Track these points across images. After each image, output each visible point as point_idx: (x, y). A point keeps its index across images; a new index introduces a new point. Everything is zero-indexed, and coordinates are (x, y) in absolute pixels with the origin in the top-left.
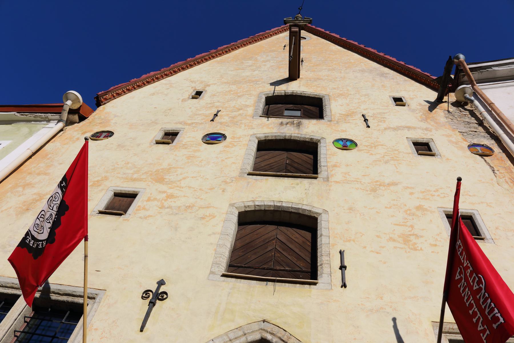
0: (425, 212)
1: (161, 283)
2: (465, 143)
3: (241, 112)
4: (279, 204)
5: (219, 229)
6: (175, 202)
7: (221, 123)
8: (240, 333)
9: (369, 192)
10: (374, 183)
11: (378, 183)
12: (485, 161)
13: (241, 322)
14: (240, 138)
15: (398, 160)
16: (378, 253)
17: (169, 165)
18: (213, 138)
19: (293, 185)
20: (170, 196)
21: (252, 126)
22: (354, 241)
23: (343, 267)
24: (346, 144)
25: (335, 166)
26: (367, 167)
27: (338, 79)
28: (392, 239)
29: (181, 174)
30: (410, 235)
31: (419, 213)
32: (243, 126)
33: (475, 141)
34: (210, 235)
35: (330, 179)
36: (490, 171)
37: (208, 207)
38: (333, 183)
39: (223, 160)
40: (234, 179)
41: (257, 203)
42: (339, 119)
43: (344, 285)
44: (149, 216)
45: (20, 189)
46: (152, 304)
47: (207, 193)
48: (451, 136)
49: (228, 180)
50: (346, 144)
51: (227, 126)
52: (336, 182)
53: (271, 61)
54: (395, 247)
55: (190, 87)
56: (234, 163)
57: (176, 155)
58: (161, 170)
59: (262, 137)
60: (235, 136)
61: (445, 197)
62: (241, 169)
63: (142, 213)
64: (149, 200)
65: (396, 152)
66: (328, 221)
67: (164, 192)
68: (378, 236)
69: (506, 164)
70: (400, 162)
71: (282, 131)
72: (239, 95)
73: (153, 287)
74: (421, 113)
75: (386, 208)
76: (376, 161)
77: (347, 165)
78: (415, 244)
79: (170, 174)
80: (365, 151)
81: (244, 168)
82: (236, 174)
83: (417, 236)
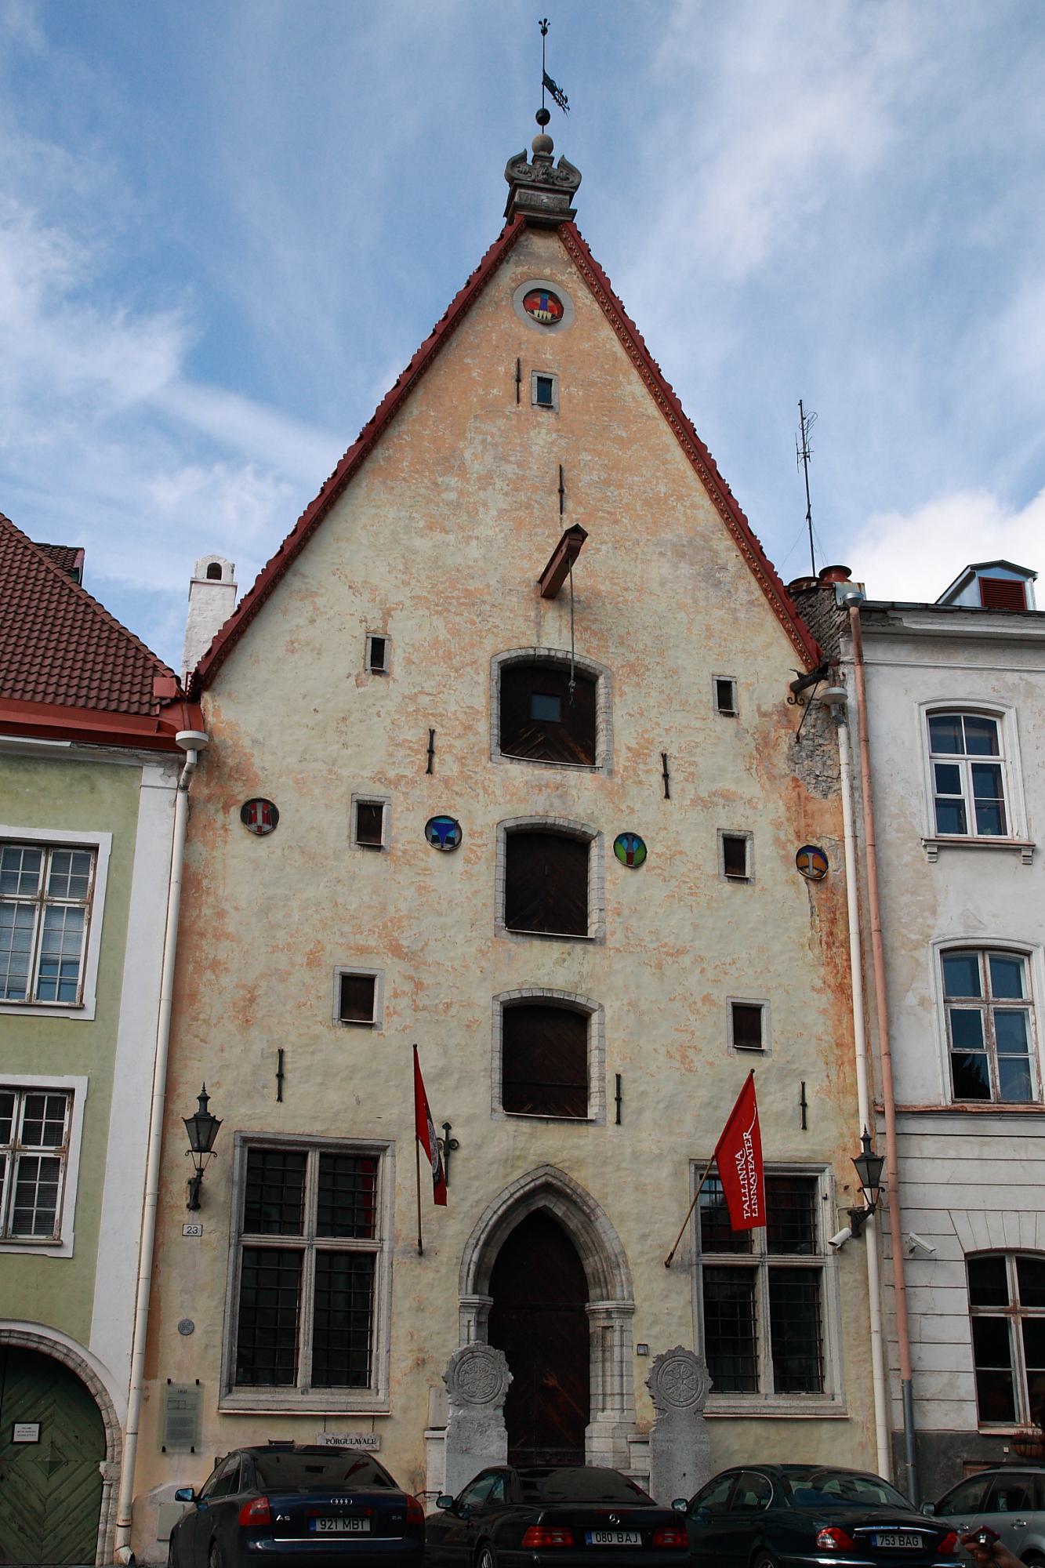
7: (446, 782)
14: (481, 834)
23: (619, 1099)
27: (630, 596)
31: (704, 1010)
33: (814, 842)
42: (626, 768)
52: (618, 950)
53: (499, 484)
60: (475, 828)
64: (396, 995)
65: (697, 874)
67: (411, 978)
82: (490, 934)
83: (698, 1050)
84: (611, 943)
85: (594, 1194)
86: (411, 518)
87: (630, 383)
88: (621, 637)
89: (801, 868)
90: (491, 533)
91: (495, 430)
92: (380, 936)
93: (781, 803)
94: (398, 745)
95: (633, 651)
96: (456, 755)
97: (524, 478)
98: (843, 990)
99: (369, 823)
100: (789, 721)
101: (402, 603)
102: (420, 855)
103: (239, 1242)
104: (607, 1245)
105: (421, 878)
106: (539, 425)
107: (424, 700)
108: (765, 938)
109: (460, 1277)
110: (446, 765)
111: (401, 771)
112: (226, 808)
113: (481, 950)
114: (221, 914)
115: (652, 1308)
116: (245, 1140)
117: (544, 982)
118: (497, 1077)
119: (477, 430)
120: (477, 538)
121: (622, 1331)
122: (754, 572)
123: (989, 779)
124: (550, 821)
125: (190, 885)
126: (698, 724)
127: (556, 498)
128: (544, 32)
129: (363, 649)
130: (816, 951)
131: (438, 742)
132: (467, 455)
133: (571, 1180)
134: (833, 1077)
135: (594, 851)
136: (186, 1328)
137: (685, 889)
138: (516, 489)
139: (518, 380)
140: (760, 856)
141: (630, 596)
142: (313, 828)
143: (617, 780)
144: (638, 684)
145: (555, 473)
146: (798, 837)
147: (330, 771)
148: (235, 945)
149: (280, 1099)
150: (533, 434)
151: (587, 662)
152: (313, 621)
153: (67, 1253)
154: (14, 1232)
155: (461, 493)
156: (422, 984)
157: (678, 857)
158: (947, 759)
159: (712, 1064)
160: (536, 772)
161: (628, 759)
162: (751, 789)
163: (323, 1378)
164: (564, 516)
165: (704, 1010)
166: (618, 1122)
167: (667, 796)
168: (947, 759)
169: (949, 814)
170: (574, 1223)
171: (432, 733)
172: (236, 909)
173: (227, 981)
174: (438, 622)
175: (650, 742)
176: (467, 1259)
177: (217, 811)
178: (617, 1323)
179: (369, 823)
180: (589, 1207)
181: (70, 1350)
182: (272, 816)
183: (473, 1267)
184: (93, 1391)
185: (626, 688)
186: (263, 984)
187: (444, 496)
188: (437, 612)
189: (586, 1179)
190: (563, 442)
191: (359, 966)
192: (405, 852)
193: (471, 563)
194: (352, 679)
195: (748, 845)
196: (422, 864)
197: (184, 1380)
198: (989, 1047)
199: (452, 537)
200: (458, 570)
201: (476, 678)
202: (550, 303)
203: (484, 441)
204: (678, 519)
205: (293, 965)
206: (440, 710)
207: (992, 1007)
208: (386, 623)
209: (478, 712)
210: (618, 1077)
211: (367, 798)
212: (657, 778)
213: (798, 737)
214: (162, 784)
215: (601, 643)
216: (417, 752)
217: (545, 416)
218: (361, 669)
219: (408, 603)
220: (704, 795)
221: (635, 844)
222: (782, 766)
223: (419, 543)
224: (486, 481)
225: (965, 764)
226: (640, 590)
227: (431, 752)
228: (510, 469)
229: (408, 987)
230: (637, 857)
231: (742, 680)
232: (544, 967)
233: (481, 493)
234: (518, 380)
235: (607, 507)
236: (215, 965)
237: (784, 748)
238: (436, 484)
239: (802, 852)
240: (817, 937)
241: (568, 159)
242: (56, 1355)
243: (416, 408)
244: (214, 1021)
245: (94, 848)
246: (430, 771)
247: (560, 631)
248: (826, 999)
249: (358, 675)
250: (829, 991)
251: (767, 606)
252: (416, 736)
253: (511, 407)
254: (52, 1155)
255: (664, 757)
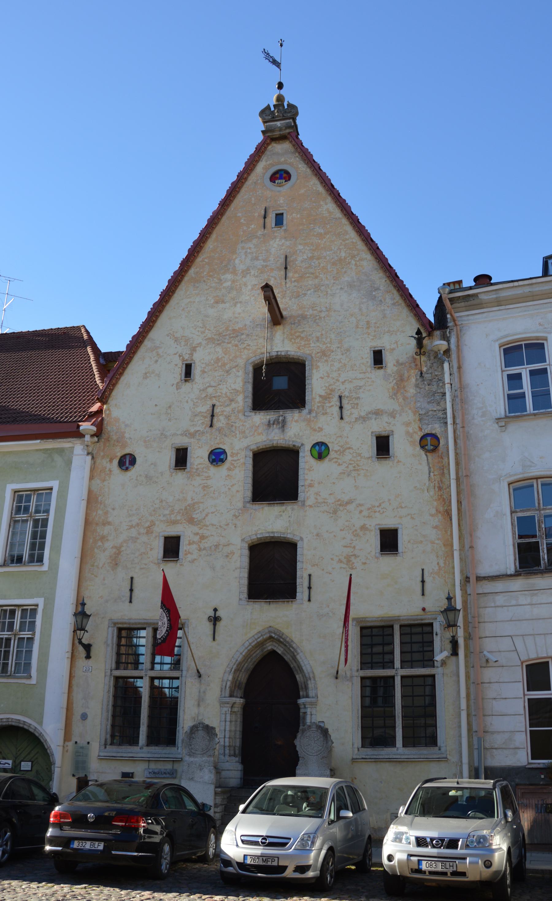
0: (366, 532)
1: (215, 610)
2: (419, 433)
3: (234, 405)
4: (272, 535)
5: (238, 564)
6: (207, 542)
7: (220, 430)
8: (260, 635)
9: (331, 515)
10: (337, 503)
11: (339, 503)
12: (428, 459)
13: (259, 629)
15: (358, 470)
16: (330, 573)
17: (192, 499)
18: (217, 457)
19: (281, 513)
20: (203, 537)
21: (244, 432)
22: (317, 565)
23: (310, 588)
24: (321, 451)
25: (311, 486)
26: (334, 483)
27: (323, 315)
28: (340, 561)
29: (203, 510)
30: (352, 555)
31: (361, 533)
32: (238, 432)
33: (427, 431)
34: (234, 571)
35: (306, 503)
36: (428, 472)
37: (228, 545)
38: (308, 507)
39: (229, 489)
40: (240, 512)
41: (259, 536)
42: (318, 407)
43: (309, 600)
44: (195, 559)
45: (100, 543)
46: (215, 625)
47: (225, 529)
48: (410, 423)
49: (237, 514)
50: (321, 451)
51: (225, 435)
52: (311, 506)
53: (253, 272)
54: (341, 568)
55: (177, 356)
56: (238, 491)
57: (194, 486)
58: (188, 507)
59: (254, 447)
60: (234, 452)
61: (383, 512)
62: (244, 498)
63: (190, 557)
64: (190, 544)
65: (359, 458)
66: (303, 548)
68: (332, 559)
69: (442, 462)
70: (359, 472)
71: (270, 438)
72: (227, 367)
73: (212, 614)
74: (395, 381)
75: (341, 530)
76: (341, 473)
77: (319, 483)
78: (353, 563)
79: (196, 512)
80: (335, 460)
81: (245, 496)
82: (240, 505)
83: (356, 556)
84: (308, 503)
85: (296, 640)
86: (207, 300)
87: (326, 204)
88: (318, 338)
89: (422, 447)
90: (248, 298)
91: (252, 246)
92: (183, 515)
93: (410, 411)
94: (196, 415)
95: (324, 343)
96: (225, 416)
97: (266, 266)
98: (448, 513)
99: (181, 458)
100: (416, 365)
101: (200, 343)
102: (204, 469)
103: (111, 674)
104: (304, 668)
105: (205, 481)
106: (275, 237)
107: (210, 390)
108: (402, 489)
109: (222, 689)
110: (220, 422)
111: (197, 428)
112: (111, 461)
113: (235, 515)
114: (106, 513)
115: (333, 703)
116: (115, 624)
117: (270, 529)
118: (245, 582)
119: (243, 248)
120: (241, 302)
121: (311, 715)
122: (395, 287)
123: (539, 376)
124: (275, 442)
125: (92, 500)
126: (362, 376)
127: (283, 272)
128: (281, 45)
129: (180, 370)
130: (432, 493)
131: (217, 410)
132: (237, 261)
133: (283, 634)
134: (442, 565)
135: (301, 454)
136: (84, 717)
137: (351, 467)
138: (262, 273)
139: (265, 217)
140: (398, 445)
141: (323, 315)
142: (152, 464)
143: (314, 414)
144: (326, 361)
145: (282, 260)
146: (421, 429)
147: (162, 434)
148: (112, 527)
149: (131, 602)
150: (271, 243)
151: (299, 354)
152: (156, 361)
153: (33, 681)
154: (14, 673)
155: (233, 281)
156: (203, 536)
157: (347, 451)
158: (514, 370)
159: (365, 563)
160: (268, 417)
161: (319, 402)
162: (391, 405)
163: (152, 740)
164: (287, 280)
165: (361, 533)
166: (309, 600)
167: (342, 418)
168: (514, 370)
169: (515, 401)
170: (287, 658)
171: (214, 406)
172: (113, 509)
173: (108, 545)
174: (219, 349)
175: (332, 390)
176: (225, 679)
177: (107, 462)
178: (309, 711)
179: (181, 458)
180: (293, 648)
181: (36, 728)
182: (133, 461)
183: (229, 683)
184: (46, 747)
185: (319, 364)
186: (125, 545)
187: (224, 285)
188: (218, 344)
189: (293, 634)
190: (288, 243)
191: (172, 531)
192: (197, 469)
193: (237, 315)
194: (175, 386)
195: (391, 438)
196: (206, 475)
197: (82, 742)
198: (541, 537)
199: (227, 305)
200: (230, 321)
201: (238, 373)
202: (284, 175)
203: (246, 252)
204: (351, 268)
205: (139, 534)
206: (219, 394)
207: (542, 512)
208: (192, 354)
209: (238, 391)
210: (310, 575)
211: (179, 445)
212: (336, 409)
213: (421, 373)
214: (82, 453)
215: (307, 343)
216: (205, 417)
217: (279, 232)
218: (179, 381)
219: (204, 342)
220: (363, 414)
221: (323, 448)
222: (412, 391)
223: (211, 312)
224: (246, 272)
225: (525, 371)
226: (329, 310)
227: (213, 416)
228: (259, 263)
229: (197, 538)
230: (323, 455)
231: (388, 347)
232: (273, 520)
233: (244, 280)
234: (265, 217)
235: (311, 270)
236: (103, 538)
237: (413, 380)
238: (220, 280)
239: (422, 438)
240: (432, 485)
241: (291, 102)
242: (31, 730)
243: (210, 244)
244: (101, 565)
245: (51, 489)
246: (211, 426)
247: (283, 341)
248: (437, 520)
249: (178, 383)
250: (440, 515)
251: (403, 304)
252: (205, 408)
253: (260, 232)
254: (30, 636)
255: (340, 397)
